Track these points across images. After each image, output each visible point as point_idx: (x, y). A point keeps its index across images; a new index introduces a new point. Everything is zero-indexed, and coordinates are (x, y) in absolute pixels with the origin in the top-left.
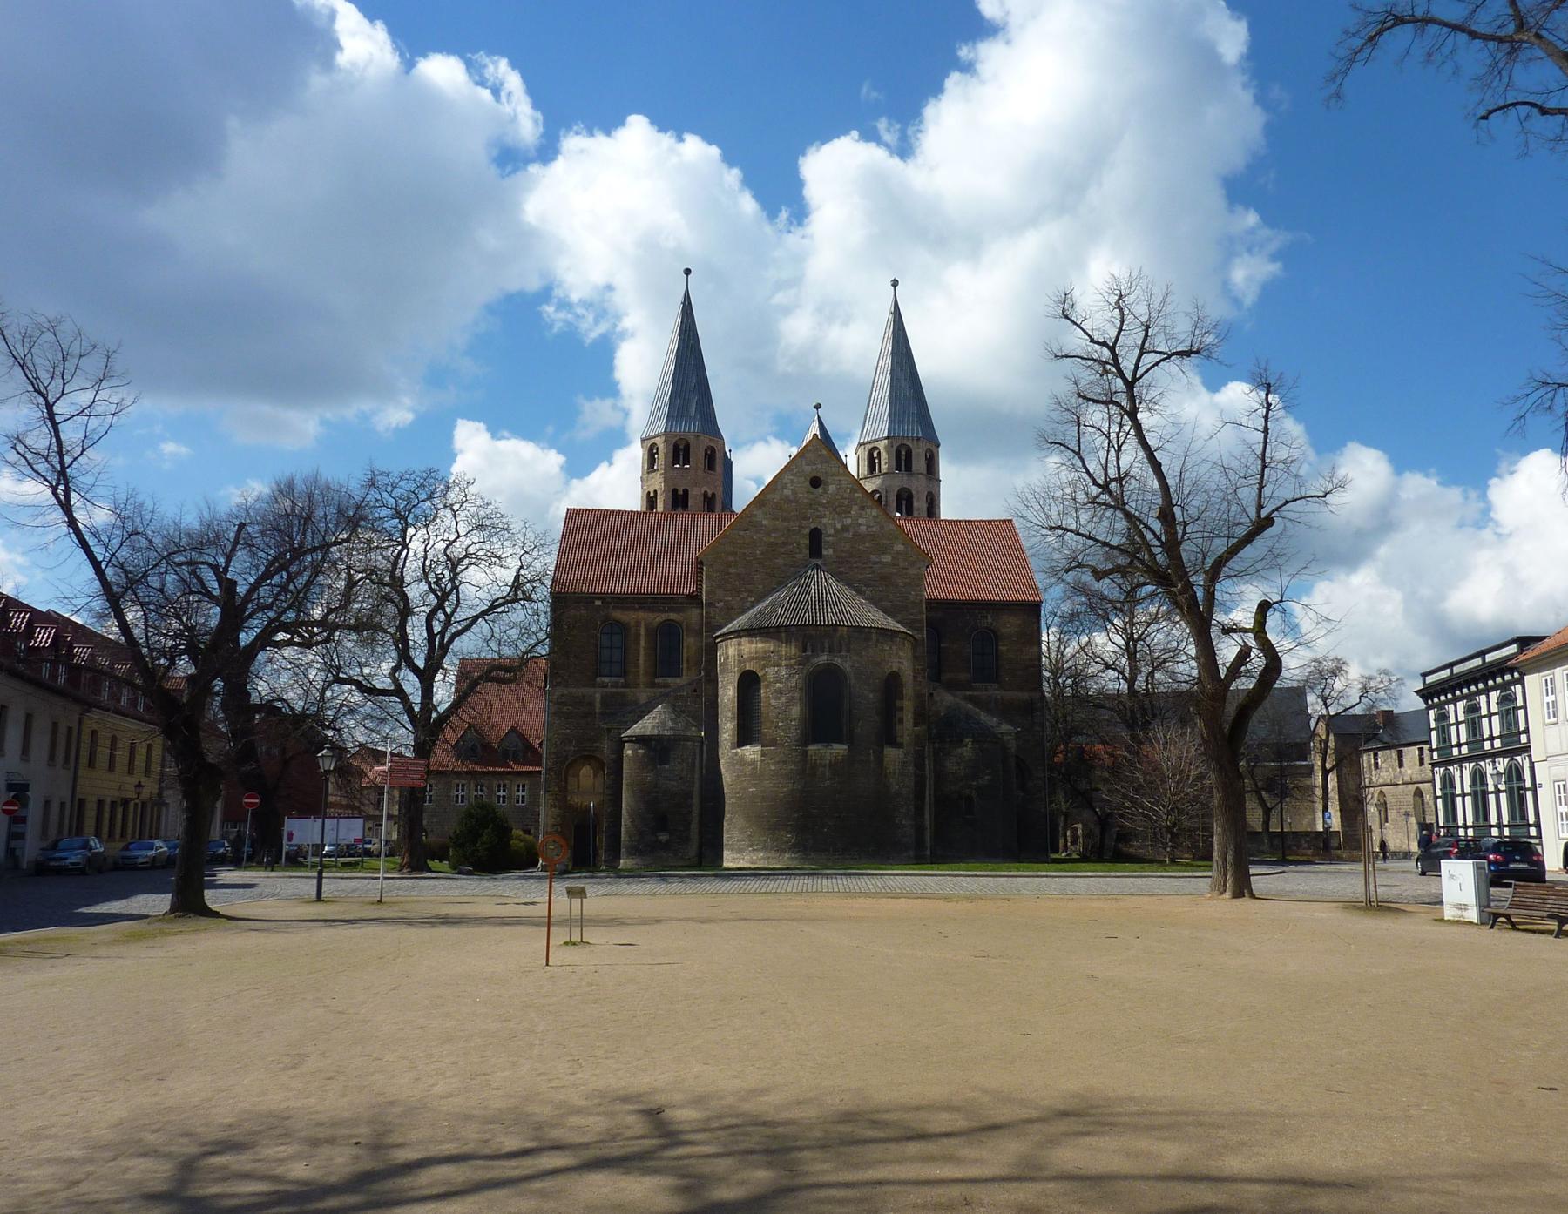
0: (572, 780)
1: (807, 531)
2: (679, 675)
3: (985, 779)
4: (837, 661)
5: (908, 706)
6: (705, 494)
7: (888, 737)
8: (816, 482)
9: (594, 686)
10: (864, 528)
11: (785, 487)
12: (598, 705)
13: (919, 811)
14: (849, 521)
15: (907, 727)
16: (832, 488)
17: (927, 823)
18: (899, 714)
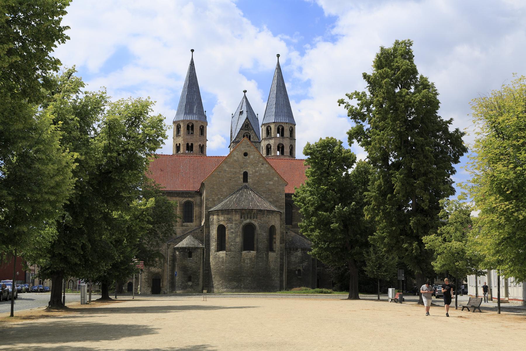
1: (242, 173)
2: (191, 221)
3: (305, 264)
4: (253, 222)
5: (278, 238)
6: (200, 145)
7: (271, 248)
8: (246, 154)
10: (263, 171)
11: (234, 156)
13: (281, 275)
14: (258, 169)
15: (277, 244)
16: (252, 157)
17: (284, 279)
18: (274, 240)
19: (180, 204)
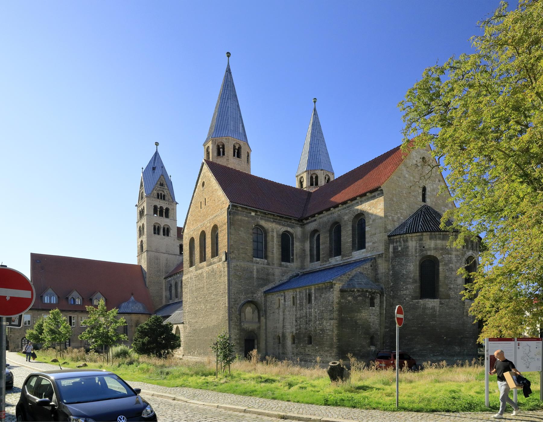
0: (242, 314)
9: (252, 261)
12: (255, 273)
19: (277, 234)
